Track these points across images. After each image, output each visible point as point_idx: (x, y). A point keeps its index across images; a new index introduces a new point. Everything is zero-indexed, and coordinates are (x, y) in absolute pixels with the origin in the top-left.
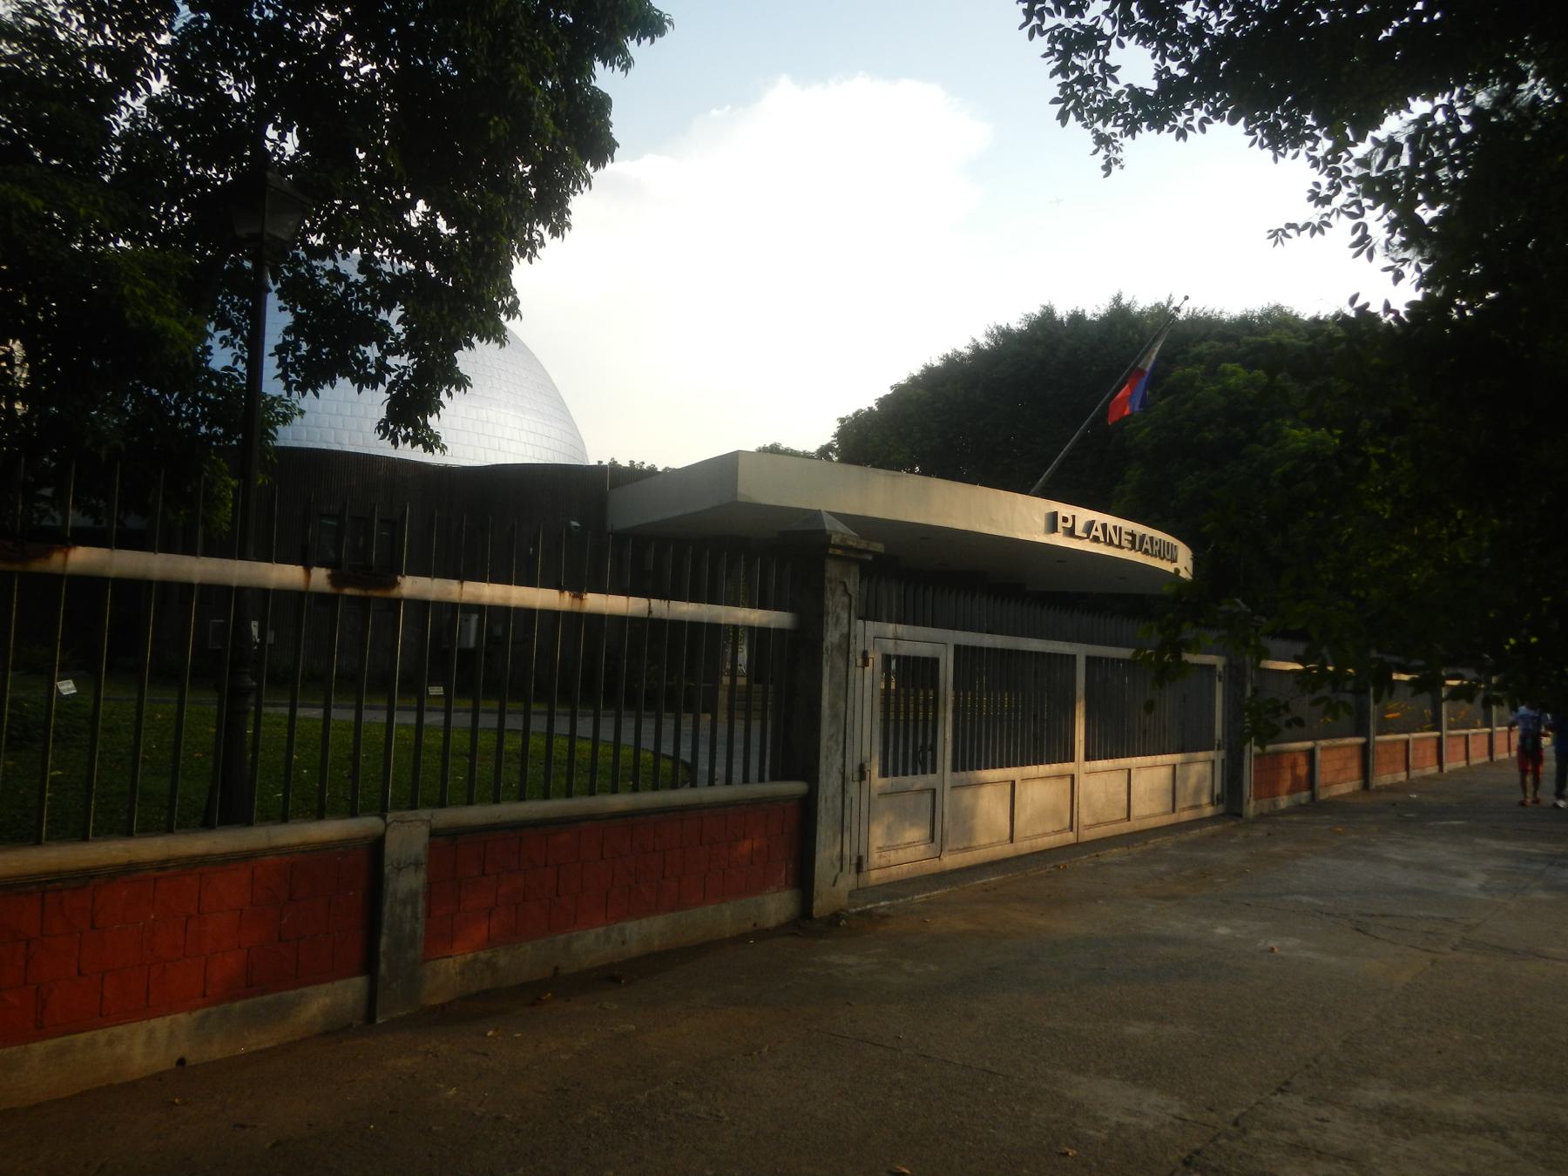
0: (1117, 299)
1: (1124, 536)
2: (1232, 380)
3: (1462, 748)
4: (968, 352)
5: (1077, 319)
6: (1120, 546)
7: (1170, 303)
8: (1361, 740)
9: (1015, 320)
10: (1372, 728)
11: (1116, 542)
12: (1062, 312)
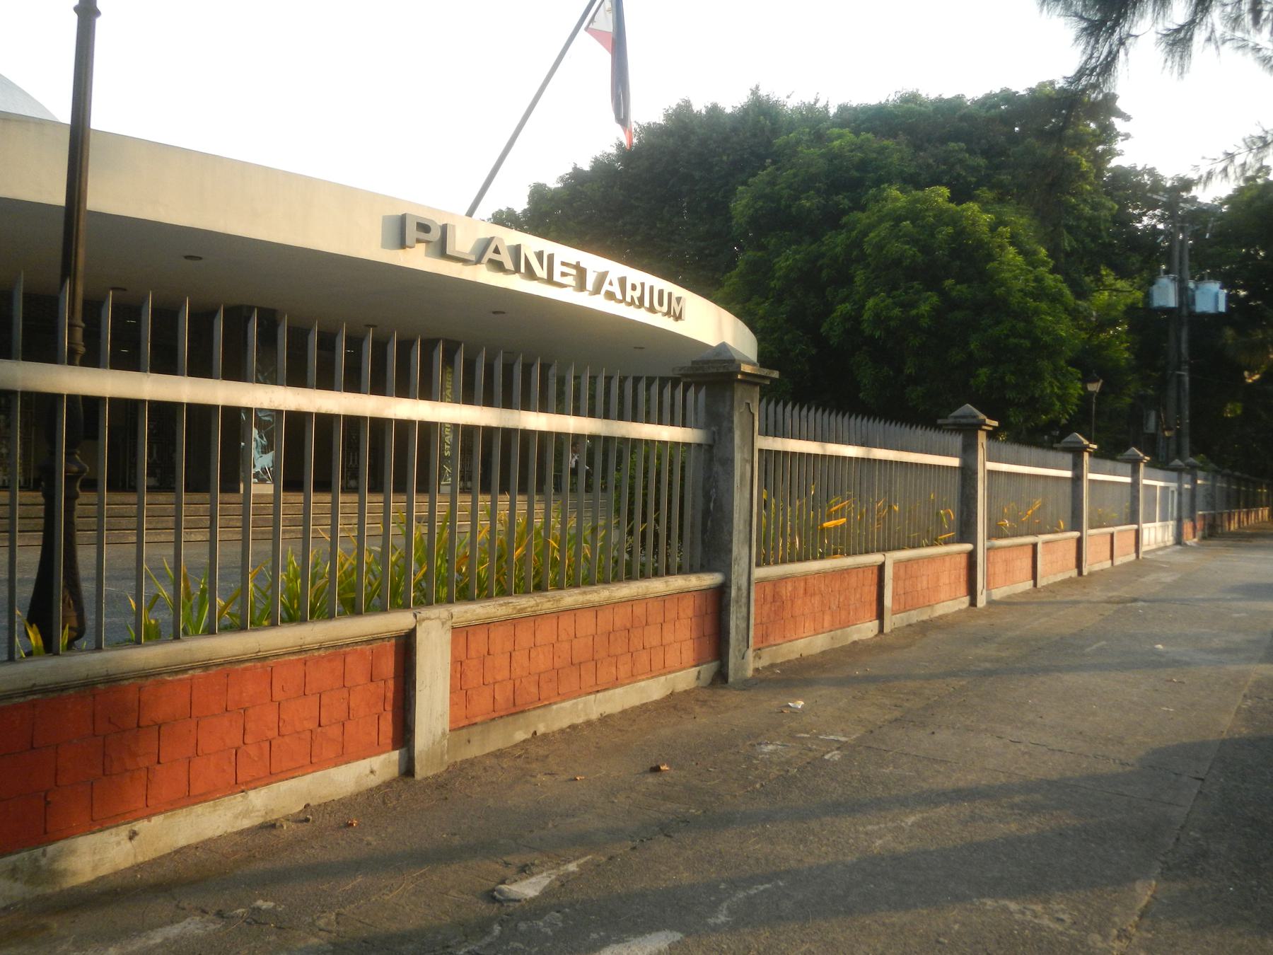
0: (755, 92)
1: (558, 269)
2: (836, 143)
3: (1027, 562)
4: (613, 151)
5: (714, 111)
6: (550, 280)
7: (817, 101)
10: (740, 551)
11: (541, 273)
12: (700, 106)
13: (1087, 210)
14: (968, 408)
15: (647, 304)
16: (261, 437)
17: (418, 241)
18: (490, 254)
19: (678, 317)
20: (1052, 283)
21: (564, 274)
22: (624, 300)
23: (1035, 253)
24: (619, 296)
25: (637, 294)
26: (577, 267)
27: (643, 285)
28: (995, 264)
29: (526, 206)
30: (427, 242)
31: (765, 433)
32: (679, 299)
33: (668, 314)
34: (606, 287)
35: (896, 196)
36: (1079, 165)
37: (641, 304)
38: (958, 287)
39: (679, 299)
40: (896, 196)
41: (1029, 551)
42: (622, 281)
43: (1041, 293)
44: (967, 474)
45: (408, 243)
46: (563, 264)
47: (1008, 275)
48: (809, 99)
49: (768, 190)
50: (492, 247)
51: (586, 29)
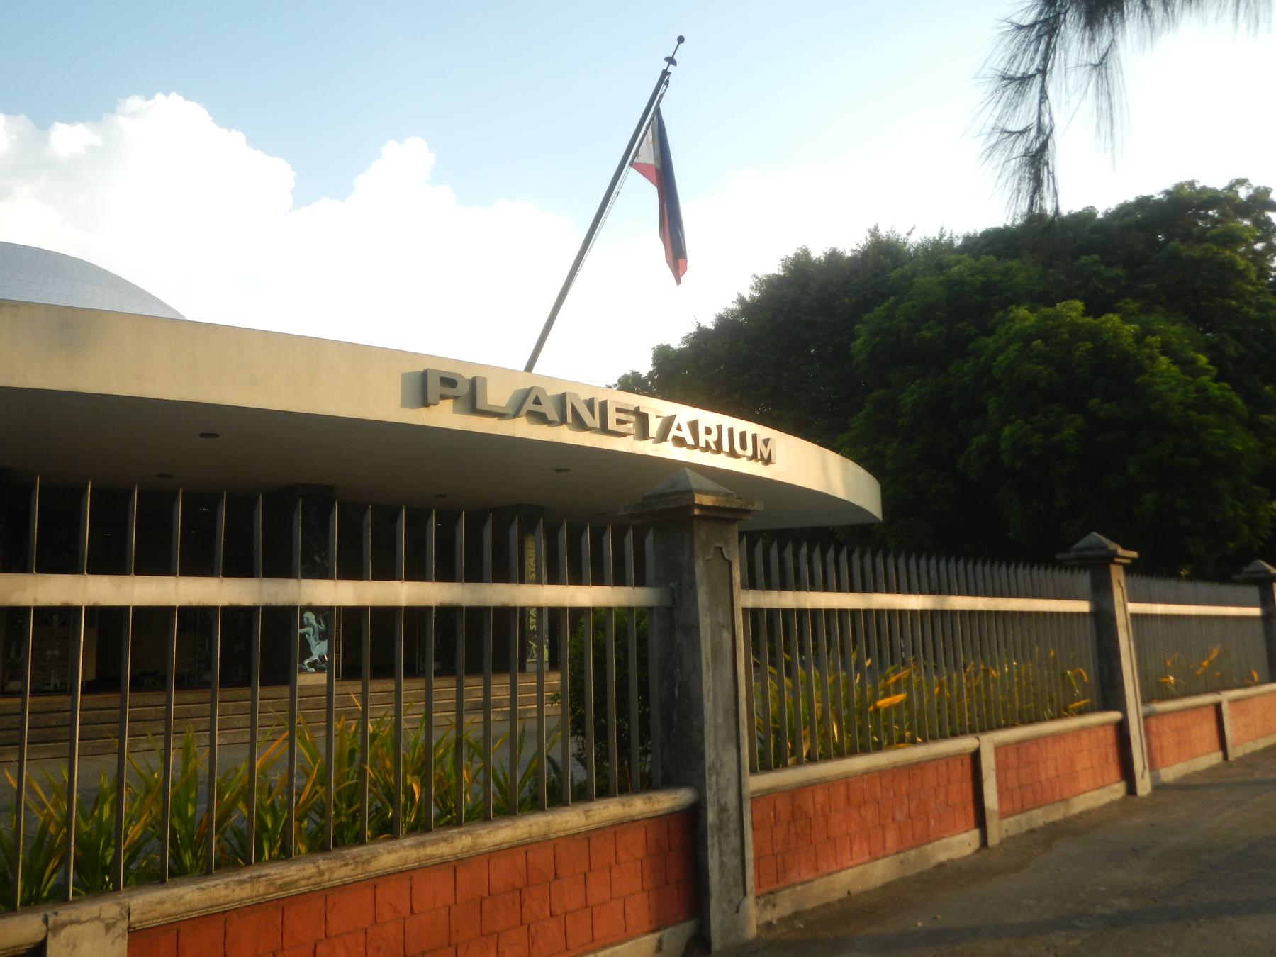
0: (874, 233)
2: (955, 269)
3: (1210, 729)
5: (834, 256)
6: (604, 429)
8: (667, 801)
9: (773, 267)
10: (721, 754)
12: (817, 253)
13: (1253, 313)
14: (1096, 537)
15: (726, 447)
16: (318, 622)
17: (443, 397)
18: (529, 405)
19: (768, 461)
20: (1217, 393)
21: (620, 422)
22: (696, 446)
23: (1194, 361)
24: (690, 441)
25: (713, 437)
26: (637, 412)
27: (719, 428)
28: (1146, 377)
29: (651, 369)
30: (455, 398)
31: (751, 584)
32: (766, 442)
34: (673, 432)
35: (1024, 316)
36: (1233, 264)
37: (719, 449)
38: (1106, 406)
39: (766, 442)
40: (1024, 316)
41: (1211, 714)
42: (694, 426)
43: (1205, 403)
44: (1103, 620)
45: (431, 398)
46: (618, 410)
47: (1162, 387)
48: (933, 234)
49: (886, 325)
50: (531, 398)
51: (631, 164)
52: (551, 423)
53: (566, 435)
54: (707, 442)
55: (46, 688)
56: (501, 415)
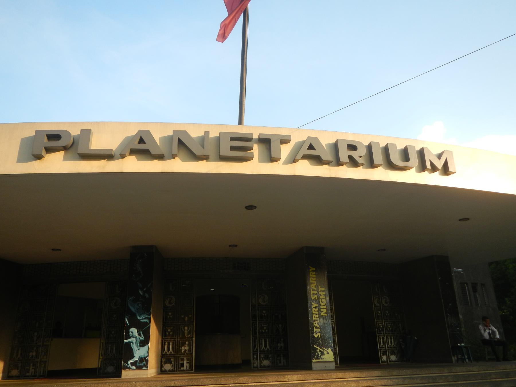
16: (139, 335)
17: (49, 150)
19: (446, 170)
22: (339, 163)
25: (362, 151)
30: (65, 148)
33: (422, 167)
46: (232, 139)
52: (161, 157)
53: (179, 166)
54: (351, 158)
55: (27, 374)
56: (108, 156)
